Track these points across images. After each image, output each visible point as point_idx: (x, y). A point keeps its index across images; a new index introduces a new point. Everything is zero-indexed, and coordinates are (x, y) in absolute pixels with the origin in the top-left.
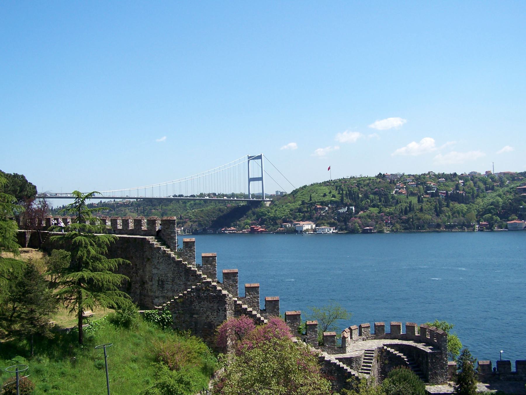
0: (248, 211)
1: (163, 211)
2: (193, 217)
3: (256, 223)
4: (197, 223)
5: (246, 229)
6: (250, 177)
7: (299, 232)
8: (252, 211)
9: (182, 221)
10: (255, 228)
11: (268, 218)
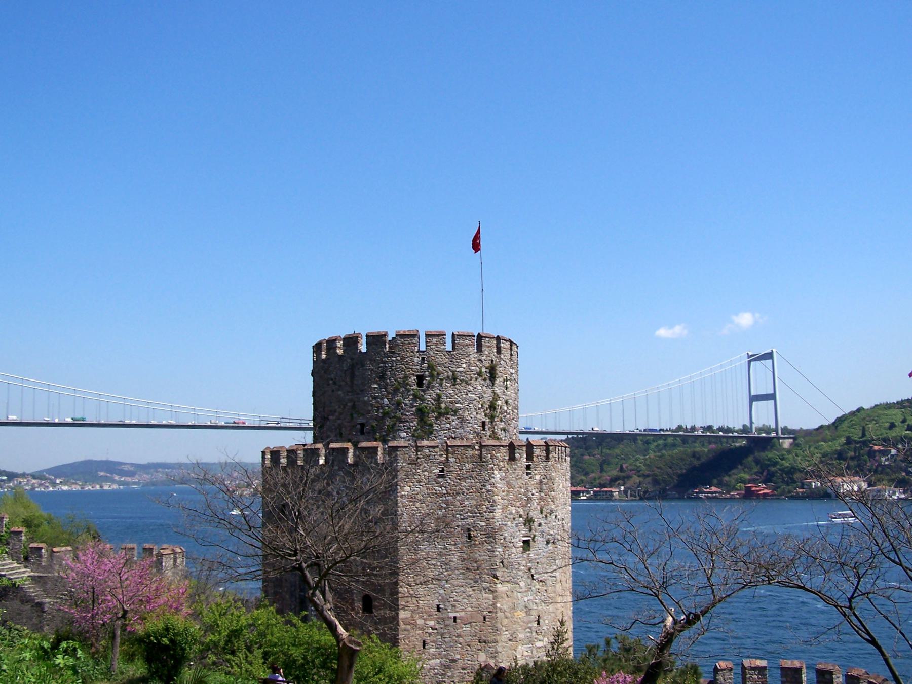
0: (746, 456)
1: (604, 458)
2: (643, 468)
3: (758, 479)
4: (649, 479)
5: (738, 490)
6: (753, 393)
7: (833, 495)
8: (754, 457)
9: (622, 474)
10: (754, 489)
11: (779, 470)
